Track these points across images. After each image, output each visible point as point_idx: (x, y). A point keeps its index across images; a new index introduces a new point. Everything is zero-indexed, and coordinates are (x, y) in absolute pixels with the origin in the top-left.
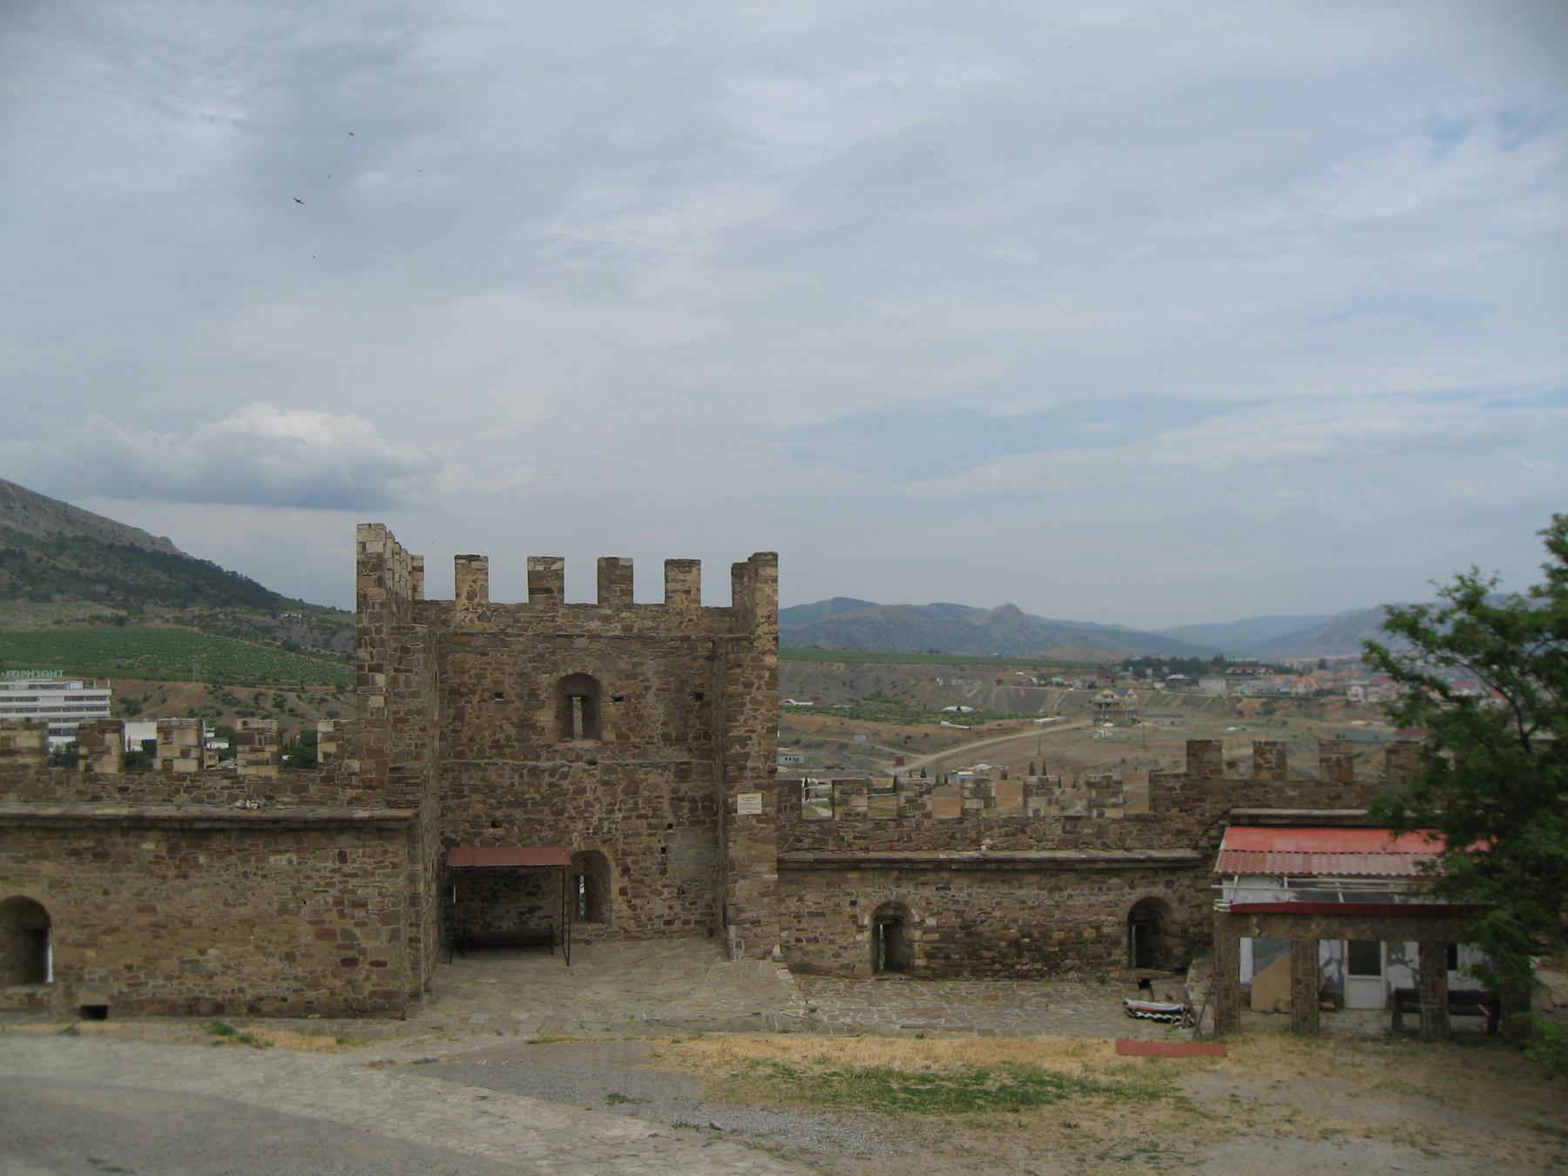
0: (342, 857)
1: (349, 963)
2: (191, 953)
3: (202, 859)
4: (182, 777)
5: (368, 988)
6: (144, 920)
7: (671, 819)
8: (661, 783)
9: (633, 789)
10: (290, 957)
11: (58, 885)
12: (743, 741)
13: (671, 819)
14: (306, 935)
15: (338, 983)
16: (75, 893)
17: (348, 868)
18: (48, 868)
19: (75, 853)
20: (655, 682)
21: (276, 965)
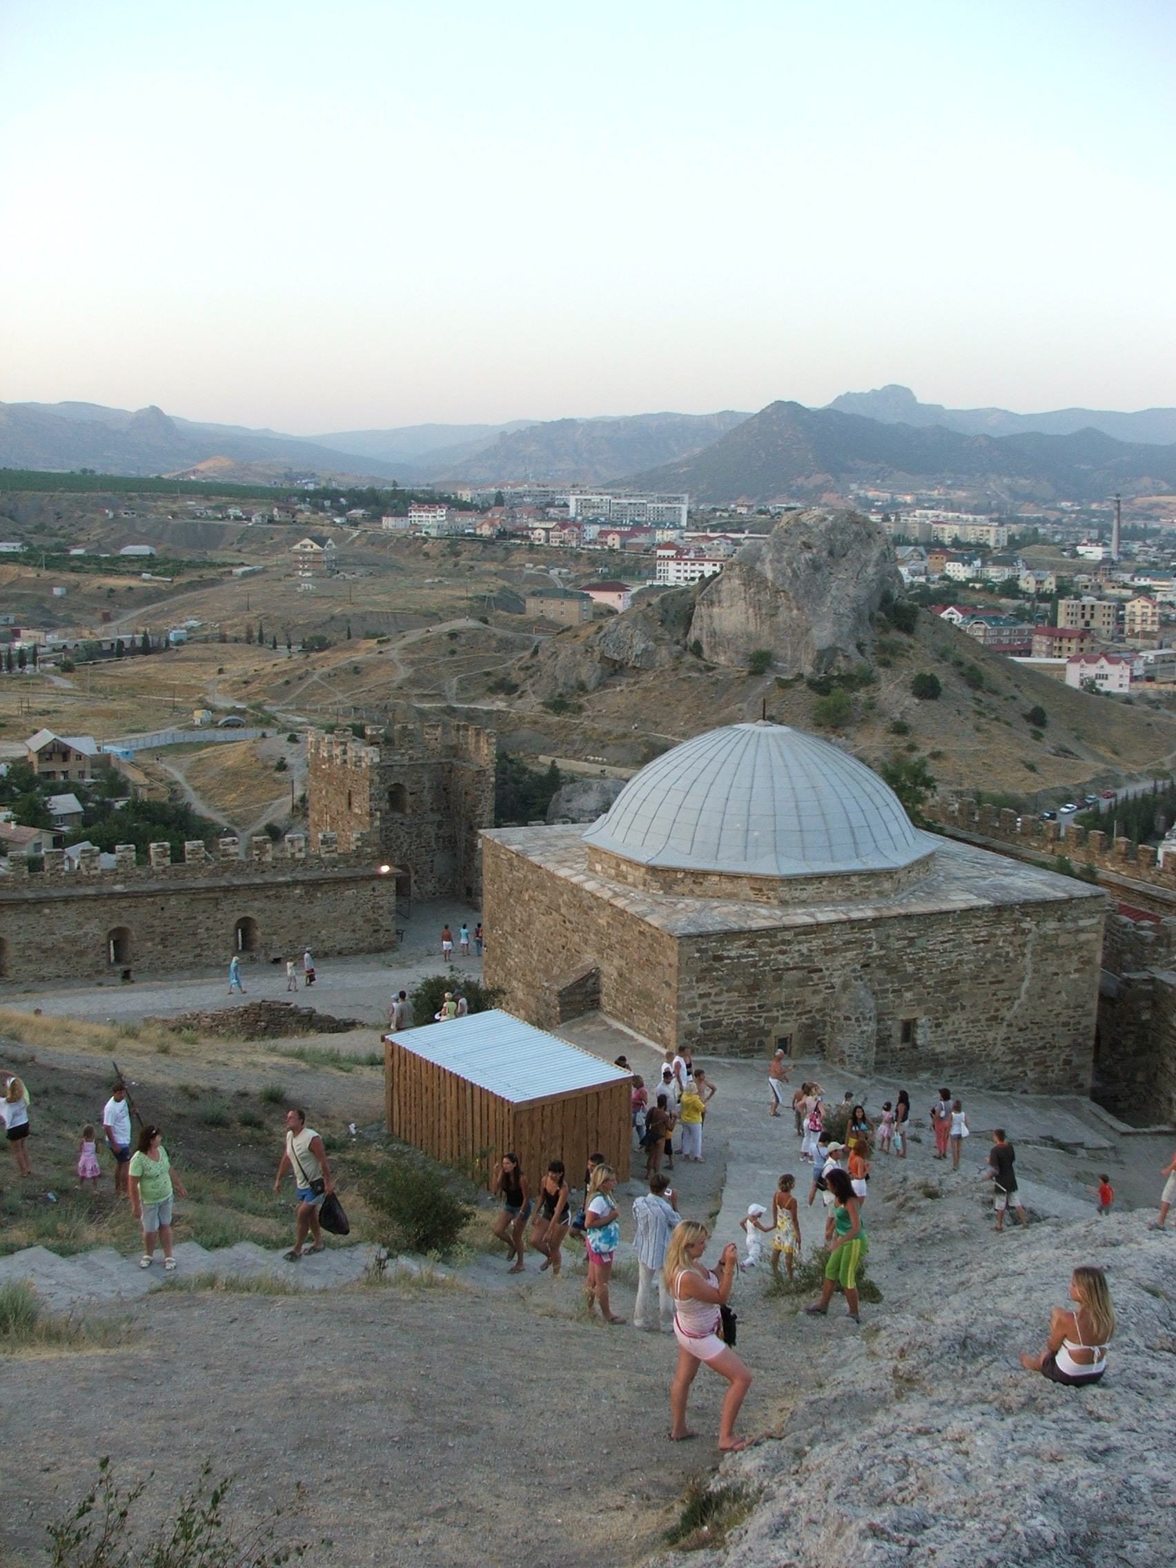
0: (374, 890)
1: (376, 931)
2: (315, 933)
3: (319, 895)
4: (299, 860)
5: (384, 940)
6: (295, 922)
7: (435, 847)
8: (431, 830)
9: (419, 836)
10: (354, 931)
11: (262, 911)
12: (481, 815)
13: (435, 847)
14: (360, 922)
15: (371, 940)
16: (268, 913)
17: (376, 894)
18: (256, 904)
19: (267, 897)
20: (427, 785)
21: (348, 935)
